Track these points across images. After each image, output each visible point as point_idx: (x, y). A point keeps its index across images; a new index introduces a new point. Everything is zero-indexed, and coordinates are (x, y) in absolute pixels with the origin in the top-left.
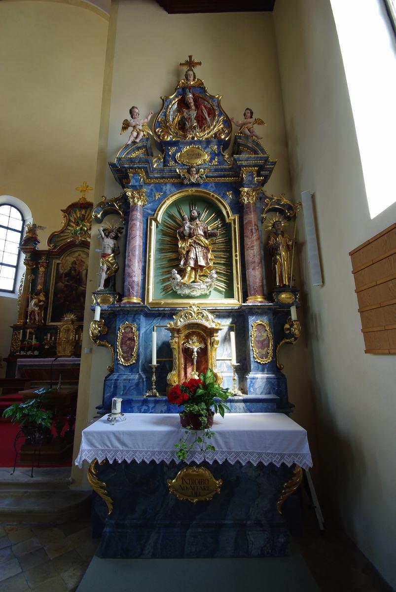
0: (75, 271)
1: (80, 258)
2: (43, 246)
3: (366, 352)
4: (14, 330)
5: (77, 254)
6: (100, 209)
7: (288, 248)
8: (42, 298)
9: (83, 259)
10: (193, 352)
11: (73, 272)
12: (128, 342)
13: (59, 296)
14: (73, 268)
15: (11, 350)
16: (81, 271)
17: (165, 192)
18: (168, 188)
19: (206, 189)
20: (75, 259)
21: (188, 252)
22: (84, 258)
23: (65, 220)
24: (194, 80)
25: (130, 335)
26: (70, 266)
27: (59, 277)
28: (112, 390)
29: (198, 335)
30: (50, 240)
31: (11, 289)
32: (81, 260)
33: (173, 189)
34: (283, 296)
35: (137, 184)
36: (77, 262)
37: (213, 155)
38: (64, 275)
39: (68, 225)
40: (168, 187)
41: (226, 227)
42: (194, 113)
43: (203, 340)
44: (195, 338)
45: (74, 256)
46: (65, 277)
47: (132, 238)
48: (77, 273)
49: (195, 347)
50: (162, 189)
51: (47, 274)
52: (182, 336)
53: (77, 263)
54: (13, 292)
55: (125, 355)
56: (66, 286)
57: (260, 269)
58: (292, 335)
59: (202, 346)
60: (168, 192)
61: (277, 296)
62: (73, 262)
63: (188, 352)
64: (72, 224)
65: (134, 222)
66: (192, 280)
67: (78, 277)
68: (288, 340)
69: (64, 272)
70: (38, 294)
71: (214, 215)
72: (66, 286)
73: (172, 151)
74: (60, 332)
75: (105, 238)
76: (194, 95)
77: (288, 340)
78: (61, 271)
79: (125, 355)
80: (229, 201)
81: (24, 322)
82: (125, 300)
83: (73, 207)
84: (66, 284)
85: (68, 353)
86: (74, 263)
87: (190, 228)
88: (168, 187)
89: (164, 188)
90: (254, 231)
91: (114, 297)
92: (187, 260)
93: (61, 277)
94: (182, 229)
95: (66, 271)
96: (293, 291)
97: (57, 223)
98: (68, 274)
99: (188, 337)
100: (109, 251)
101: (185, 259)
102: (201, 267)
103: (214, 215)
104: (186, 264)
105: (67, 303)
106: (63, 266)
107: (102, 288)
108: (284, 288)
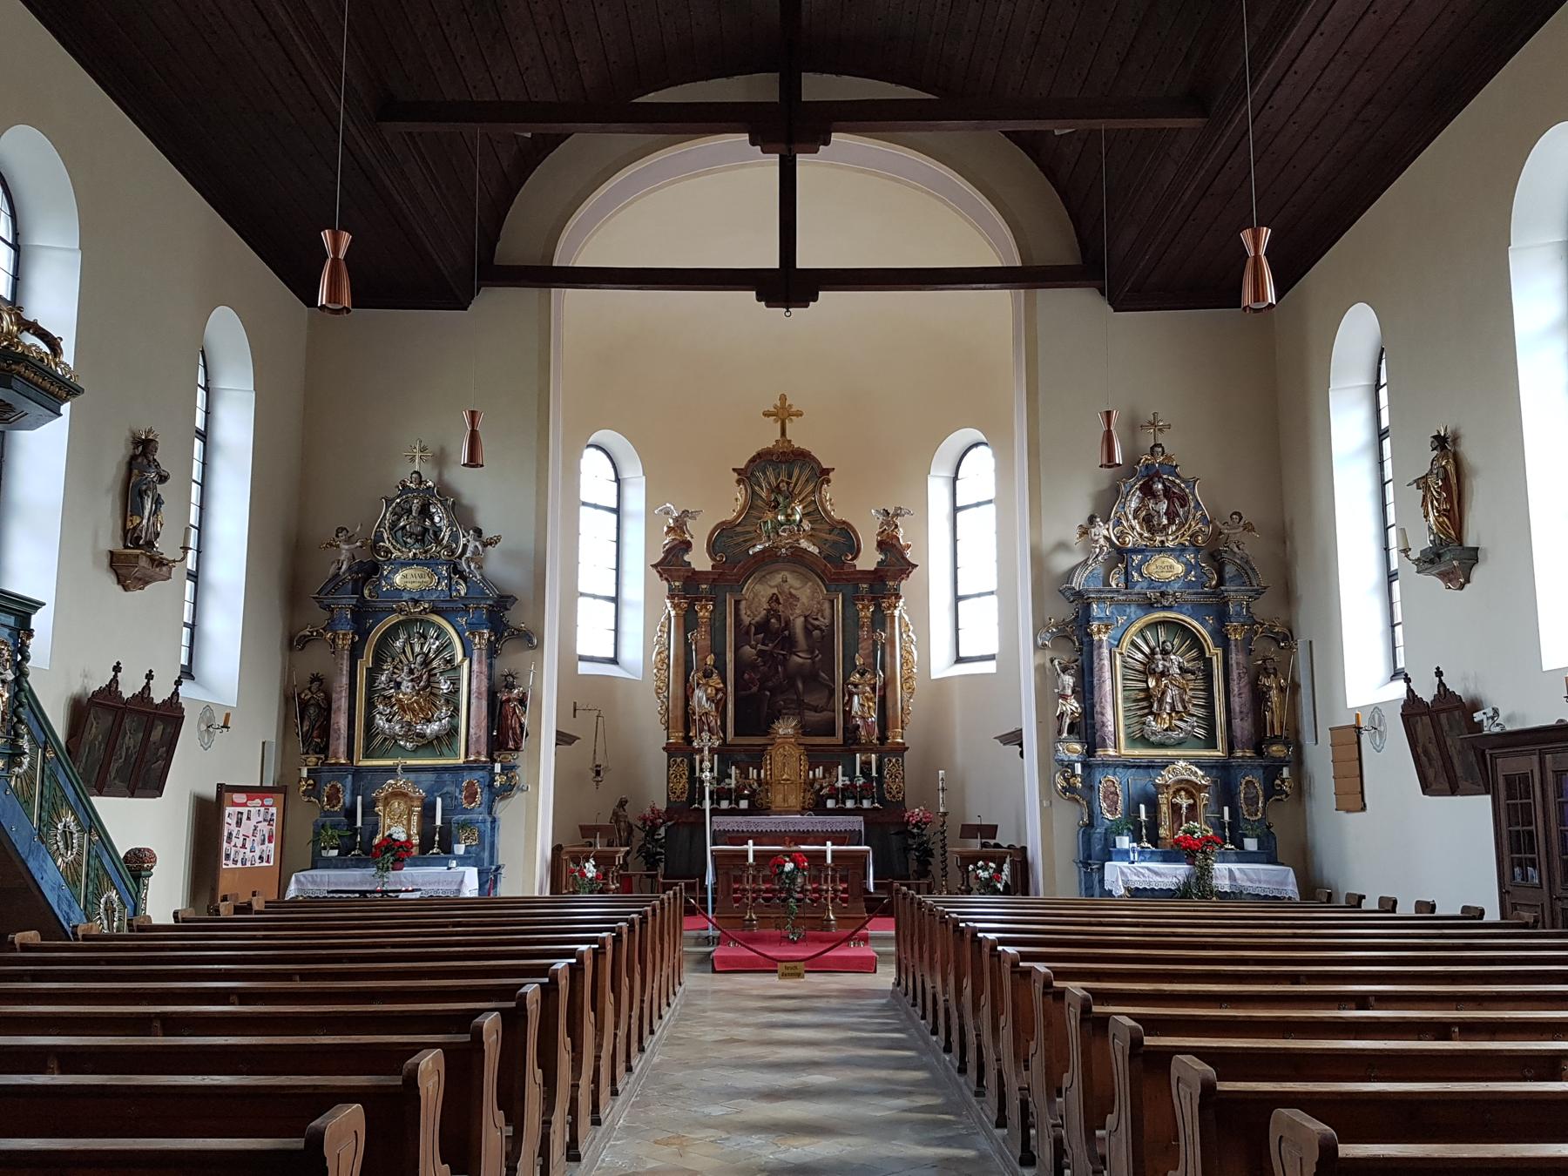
0: (779, 618)
1: (786, 587)
2: (699, 560)
3: (1336, 810)
4: (669, 758)
5: (778, 578)
6: (1048, 635)
7: (1282, 690)
8: (715, 680)
9: (793, 591)
10: (1181, 808)
11: (773, 620)
12: (1111, 796)
13: (746, 676)
14: (771, 612)
15: (668, 799)
16: (791, 618)
17: (1129, 616)
18: (1132, 610)
19: (1181, 613)
20: (775, 591)
21: (1163, 693)
22: (796, 589)
23: (743, 492)
24: (1162, 455)
25: (1113, 789)
26: (766, 606)
27: (742, 634)
28: (1103, 842)
29: (1187, 791)
30: (713, 548)
31: (611, 655)
32: (790, 593)
33: (1139, 612)
34: (1274, 748)
35: (1101, 616)
36: (779, 596)
37: (1189, 567)
38: (753, 629)
39: (751, 506)
40: (1133, 609)
41: (1208, 662)
42: (1164, 506)
43: (1190, 795)
44: (1183, 793)
45: (773, 583)
46: (755, 635)
47: (1103, 682)
48: (783, 625)
49: (1184, 802)
50: (1125, 611)
51: (717, 630)
52: (1171, 792)
53: (781, 601)
54: (614, 661)
55: (1109, 809)
56: (761, 653)
57: (1250, 720)
58: (1282, 792)
59: (1191, 801)
60: (1133, 616)
61: (1267, 747)
62: (771, 598)
63: (1175, 809)
64: (760, 503)
65: (1103, 662)
66: (1166, 726)
67: (786, 633)
68: (1278, 797)
69: (753, 622)
70: (707, 675)
71: (1188, 642)
72: (761, 653)
73: (1137, 558)
74: (770, 759)
75: (1062, 674)
76: (1164, 484)
77: (1278, 797)
78: (746, 620)
79: (1109, 809)
80: (1210, 628)
81: (683, 738)
82: (1100, 752)
83: (762, 459)
84: (761, 651)
85: (794, 800)
86: (774, 599)
87: (1164, 666)
88: (1133, 609)
89: (1128, 610)
90: (1242, 675)
91: (1083, 747)
92: (1161, 701)
93: (748, 633)
94: (1153, 666)
95: (757, 619)
96: (1287, 745)
97: (728, 503)
98: (763, 627)
99: (1177, 791)
100: (1069, 692)
101: (1159, 702)
102: (1177, 712)
103: (1188, 642)
104: (1160, 707)
105: (768, 693)
106: (749, 607)
107: (1065, 735)
108: (1275, 740)
